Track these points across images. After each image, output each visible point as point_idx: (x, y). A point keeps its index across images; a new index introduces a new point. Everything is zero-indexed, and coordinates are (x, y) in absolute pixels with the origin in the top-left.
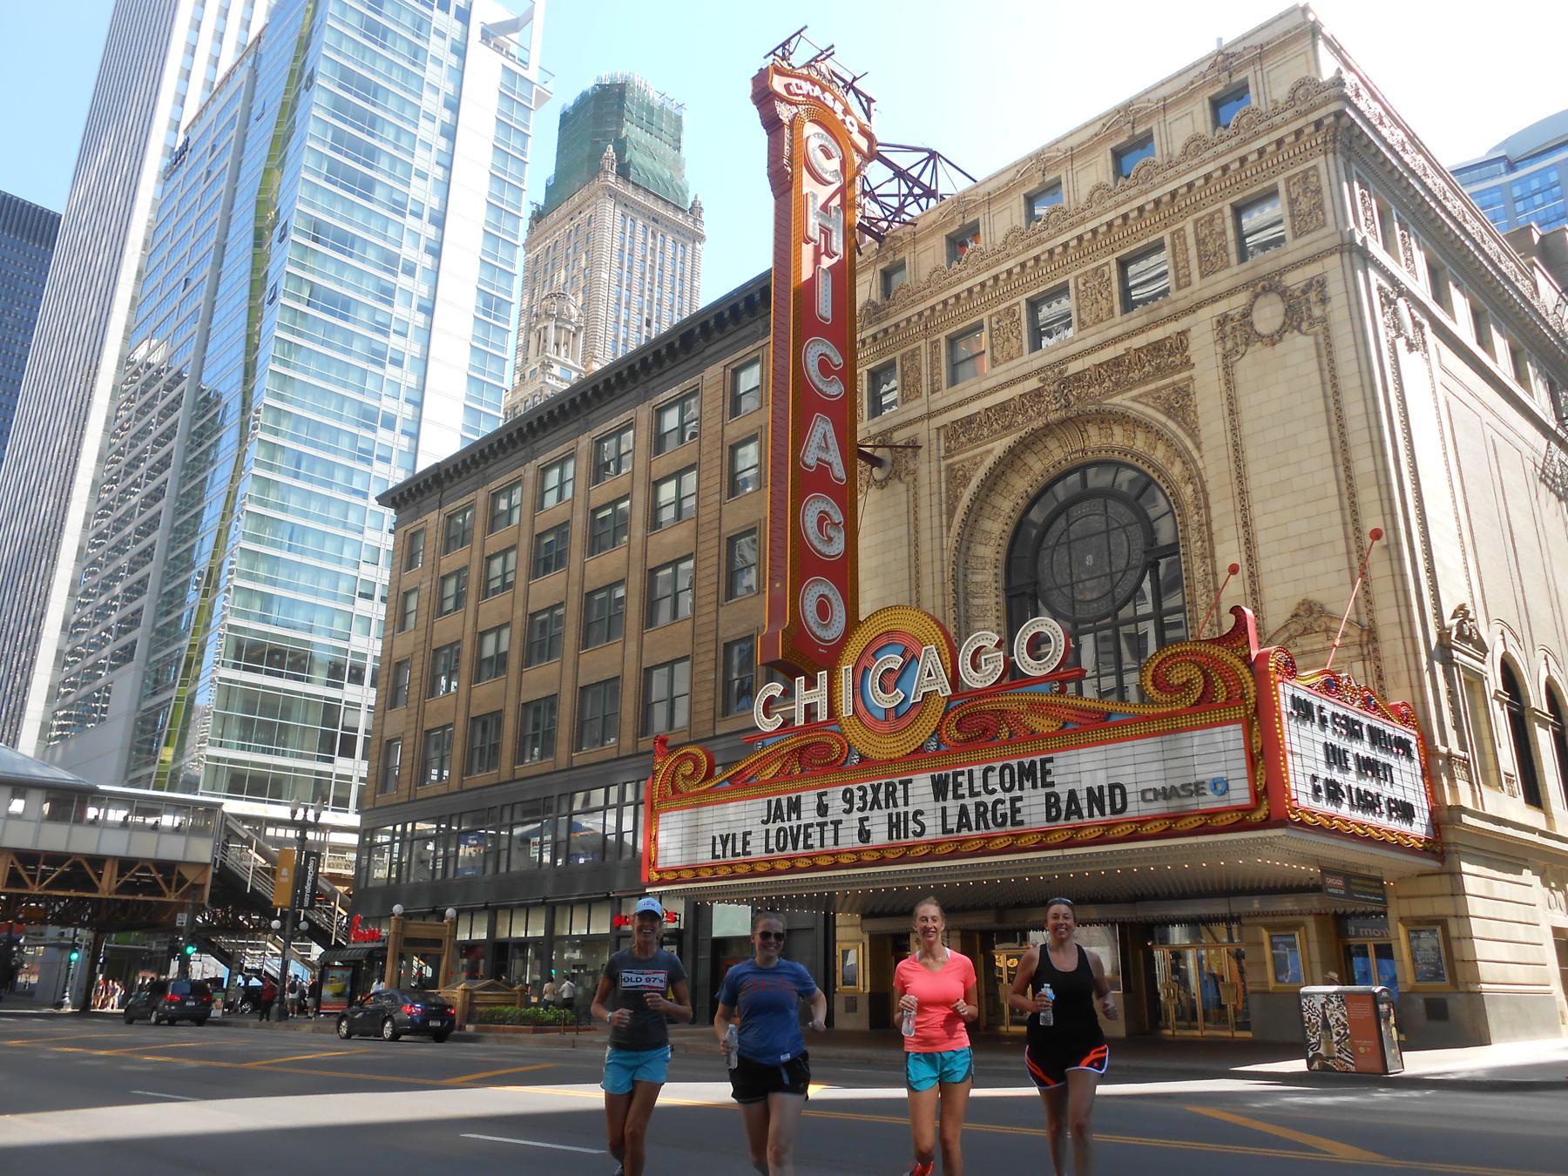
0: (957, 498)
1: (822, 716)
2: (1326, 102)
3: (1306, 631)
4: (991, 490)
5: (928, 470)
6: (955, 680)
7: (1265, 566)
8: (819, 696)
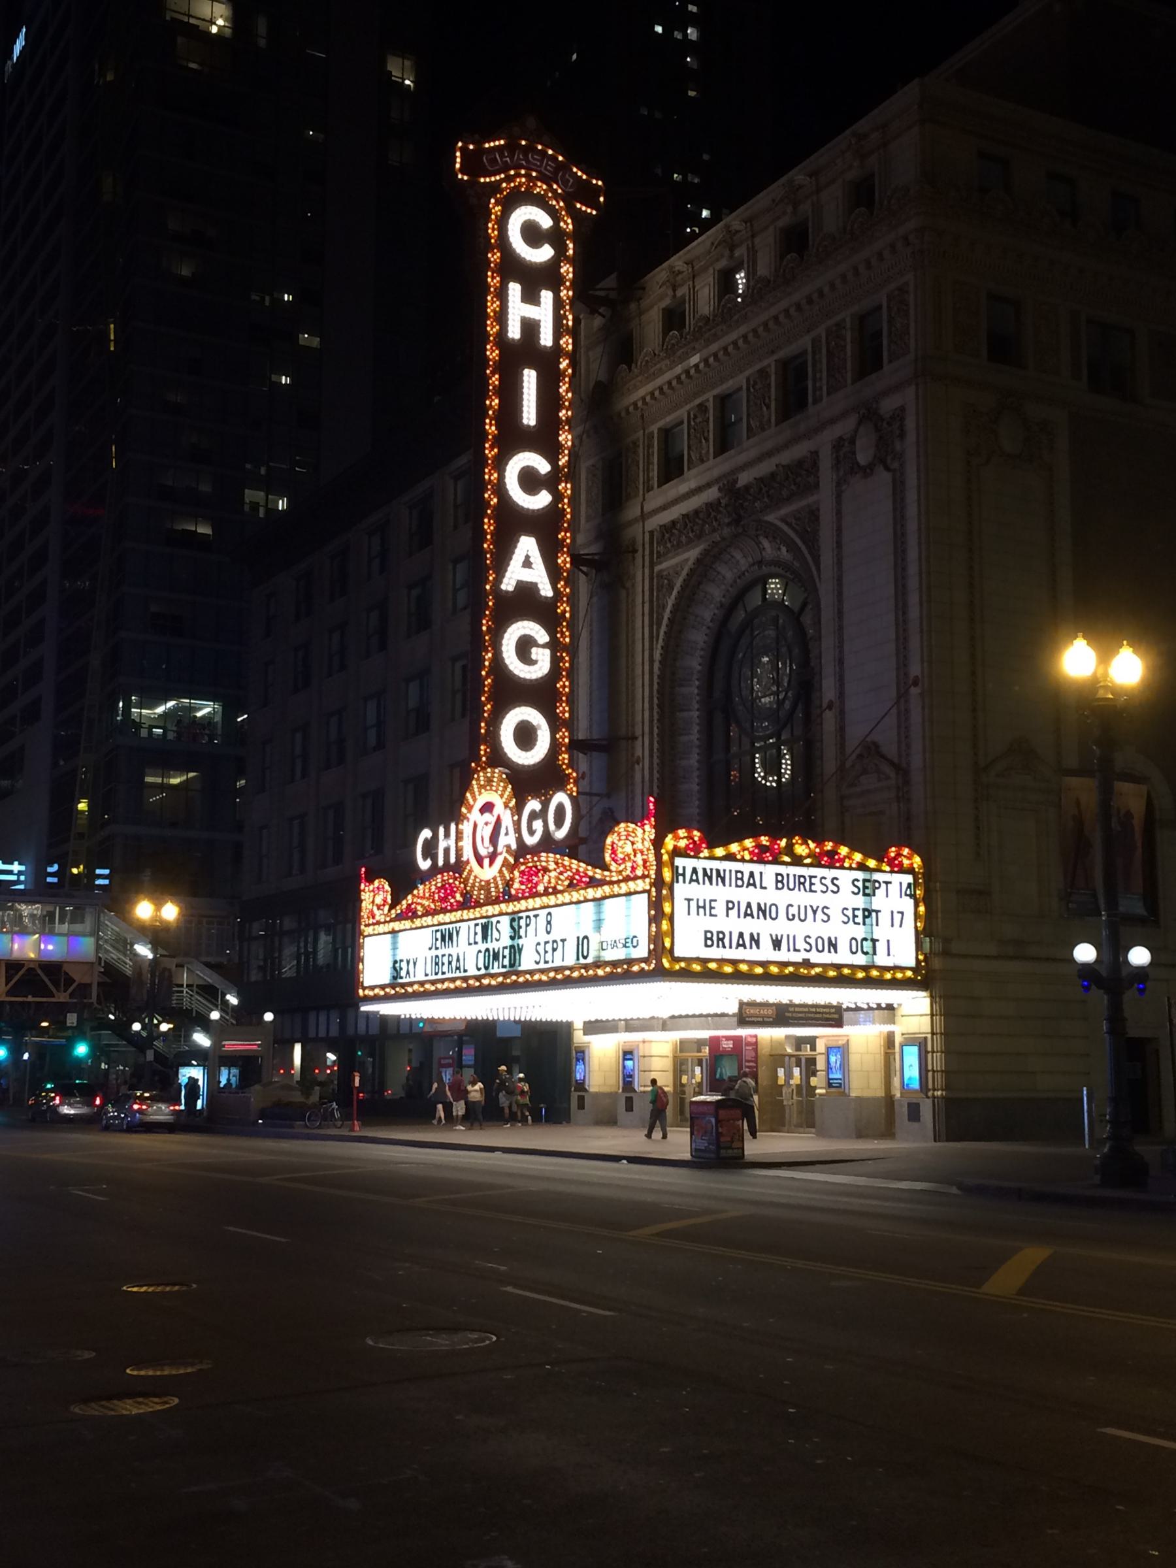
1: (453, 860)
6: (520, 840)
8: (452, 842)
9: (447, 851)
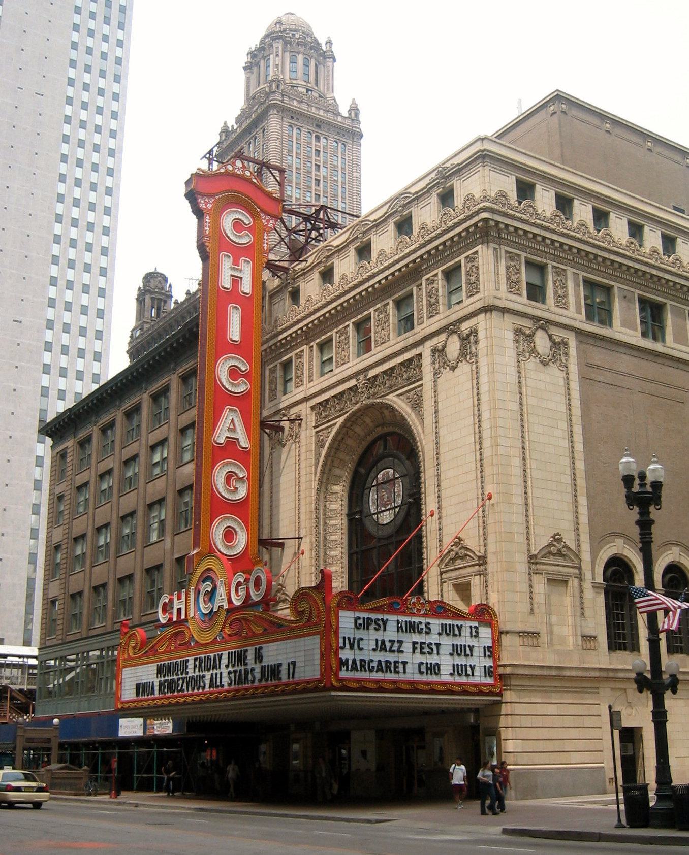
0: (320, 455)
1: (183, 617)
2: (477, 213)
3: (457, 557)
4: (337, 449)
5: (307, 434)
6: (230, 601)
7: (444, 513)
9: (179, 610)
